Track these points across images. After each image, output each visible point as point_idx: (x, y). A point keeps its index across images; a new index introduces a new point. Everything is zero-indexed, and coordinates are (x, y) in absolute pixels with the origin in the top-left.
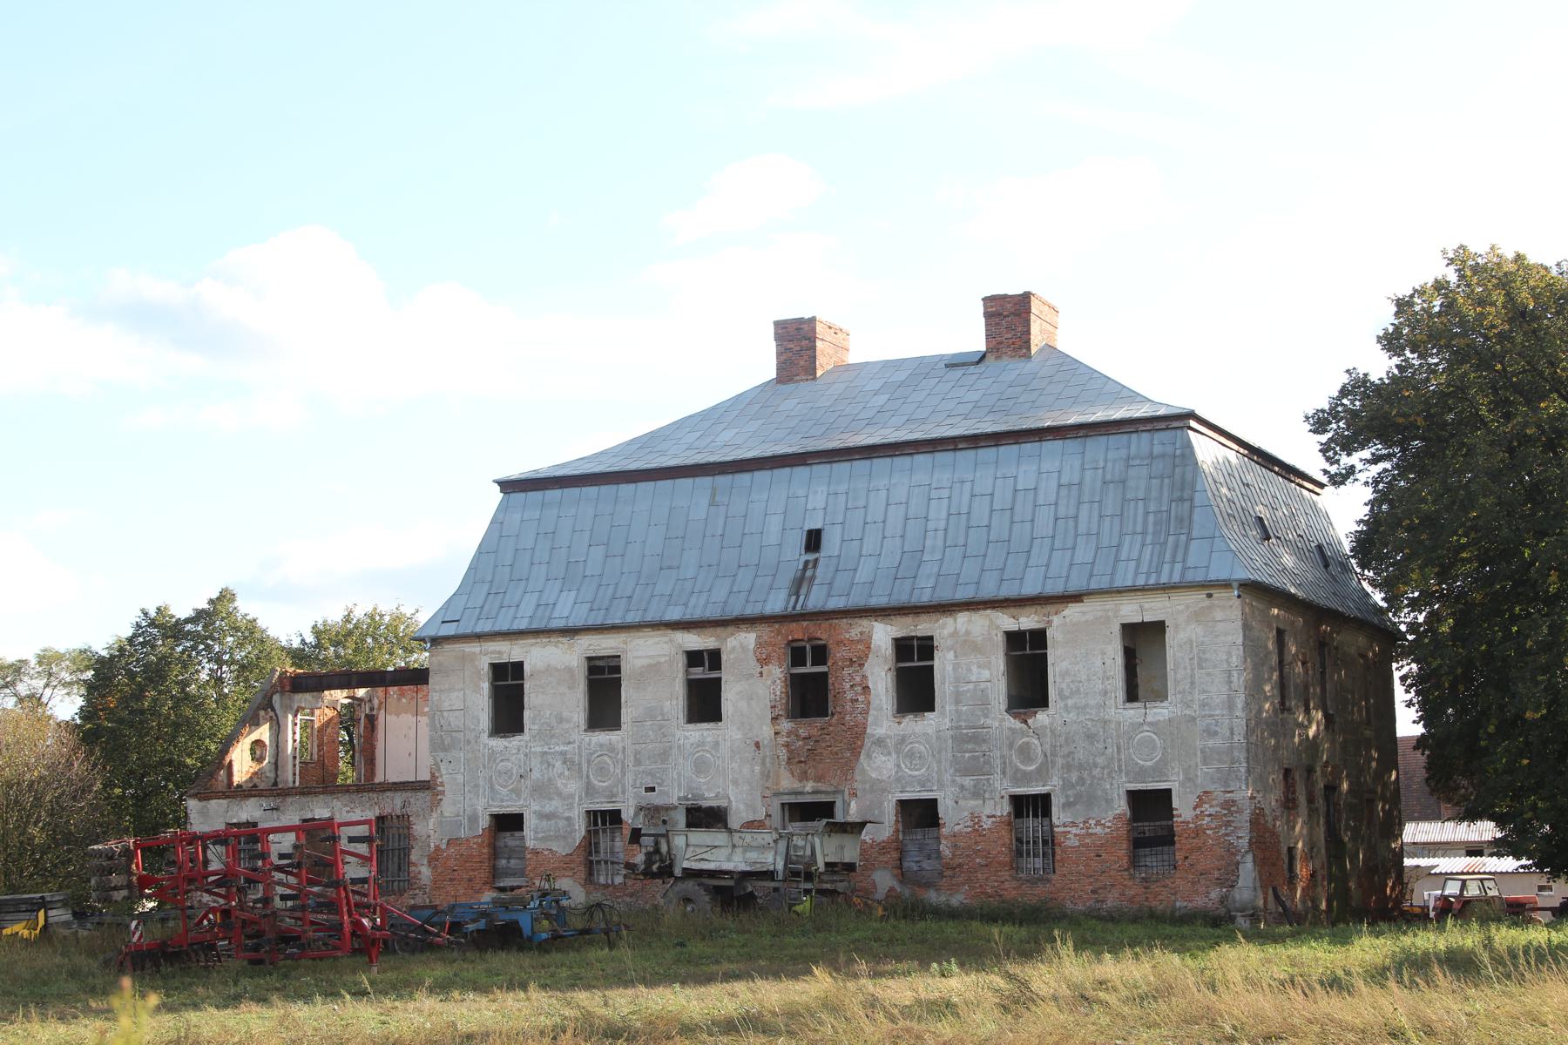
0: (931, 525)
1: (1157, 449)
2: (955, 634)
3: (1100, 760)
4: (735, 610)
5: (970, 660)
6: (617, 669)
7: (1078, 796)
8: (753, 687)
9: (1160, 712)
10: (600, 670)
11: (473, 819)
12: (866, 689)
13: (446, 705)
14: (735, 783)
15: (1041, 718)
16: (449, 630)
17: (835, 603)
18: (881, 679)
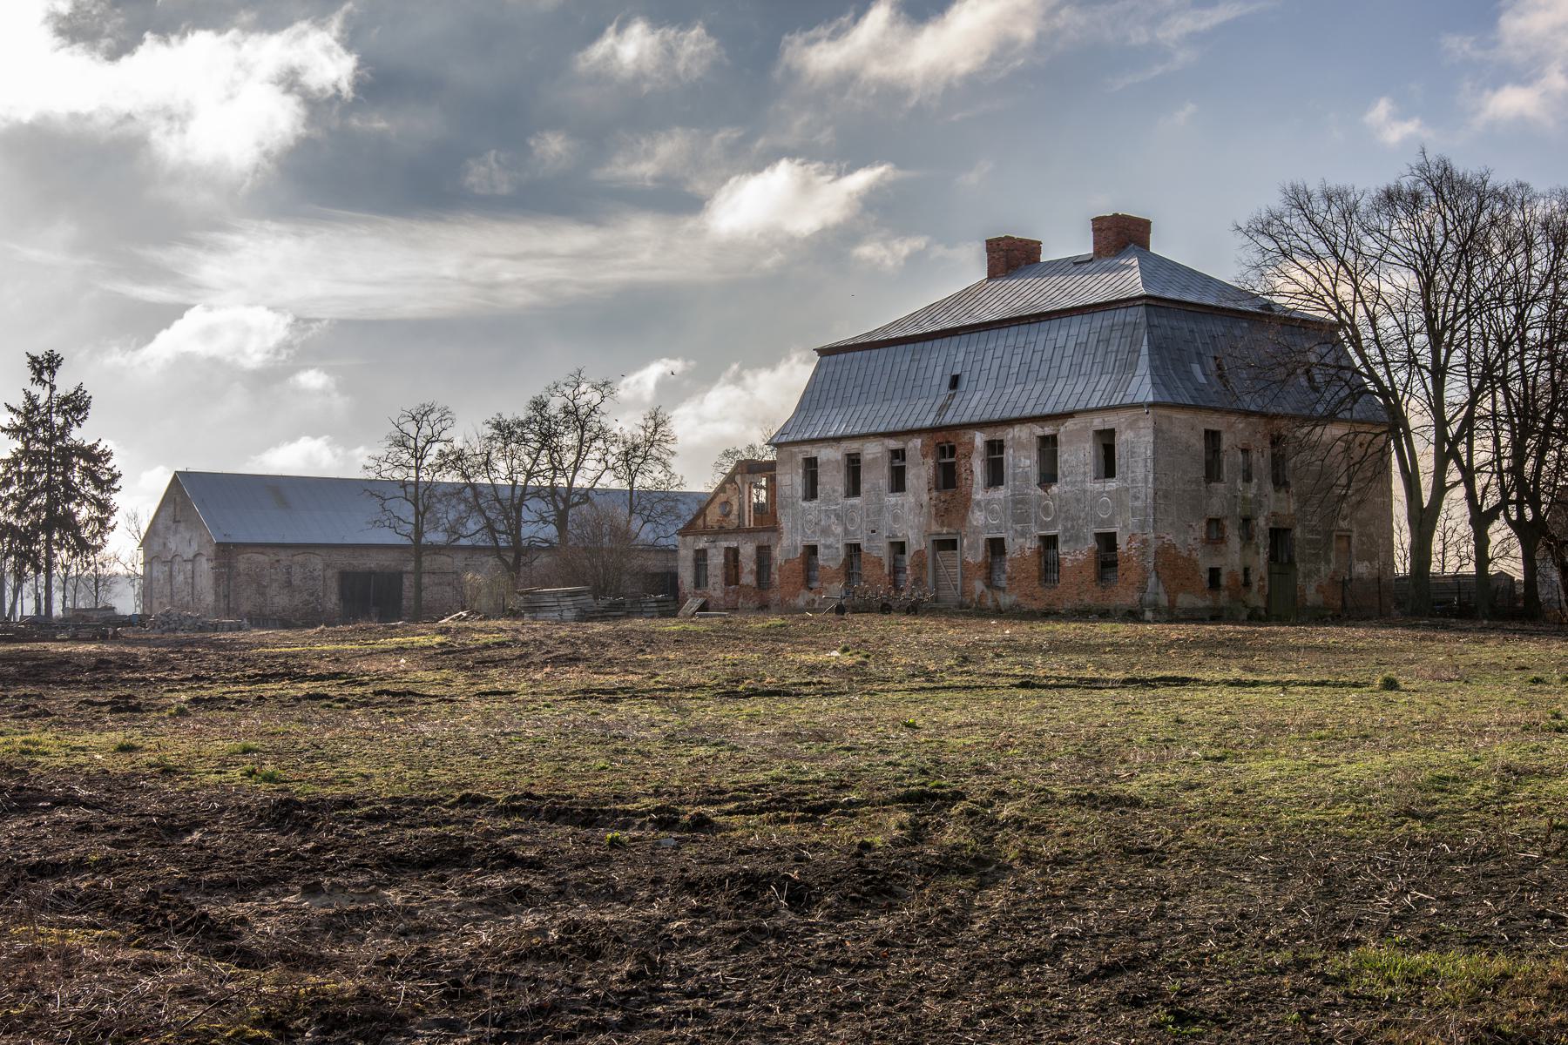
6: (859, 461)
8: (920, 474)
9: (1112, 485)
11: (796, 548)
15: (1055, 489)
16: (784, 439)
18: (978, 466)
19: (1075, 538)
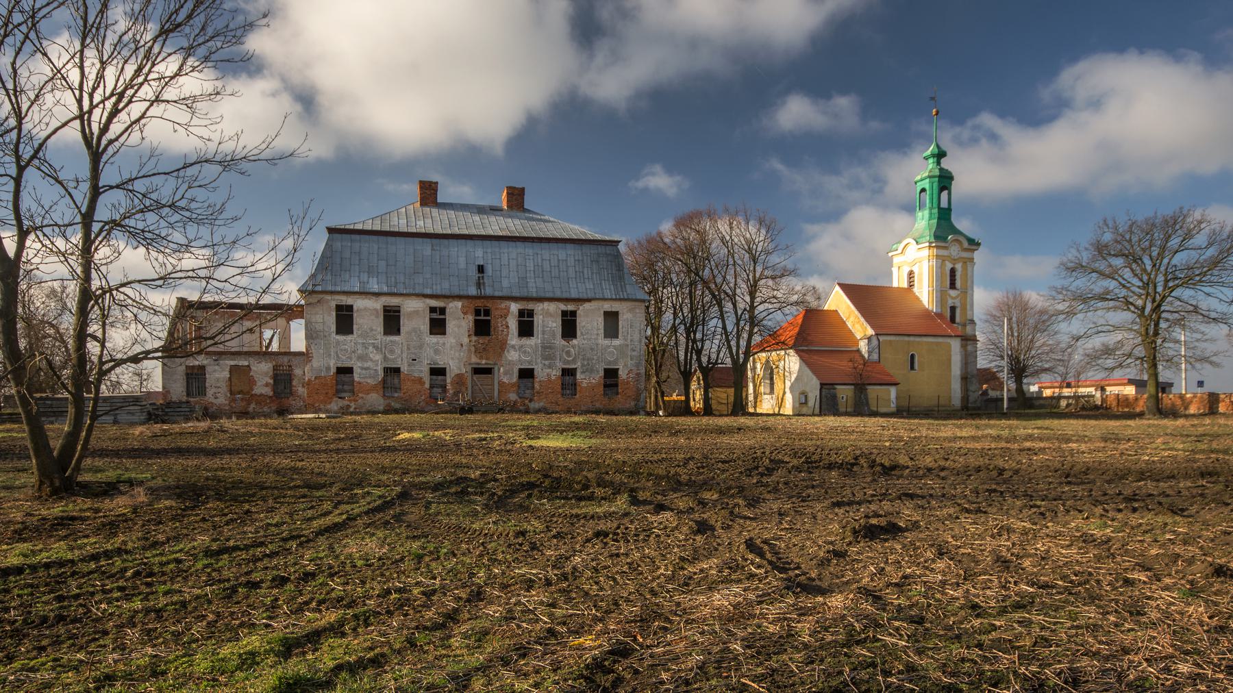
4: (456, 292)
5: (548, 319)
8: (459, 324)
9: (616, 342)
11: (328, 369)
17: (497, 294)
18: (513, 324)
19: (589, 370)
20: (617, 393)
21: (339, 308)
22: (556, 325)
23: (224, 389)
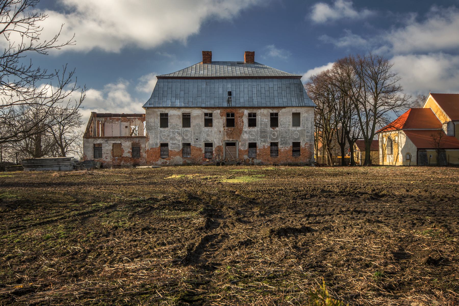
0: (254, 92)
1: (295, 82)
2: (261, 113)
3: (288, 137)
4: (217, 105)
5: (263, 117)
6: (190, 116)
7: (284, 143)
8: (219, 121)
9: (299, 129)
10: (185, 116)
11: (157, 144)
12: (243, 122)
13: (150, 121)
14: (216, 138)
15: (277, 129)
17: (237, 106)
19: (285, 143)
20: (300, 155)
21: (162, 115)
22: (267, 120)
23: (110, 154)
